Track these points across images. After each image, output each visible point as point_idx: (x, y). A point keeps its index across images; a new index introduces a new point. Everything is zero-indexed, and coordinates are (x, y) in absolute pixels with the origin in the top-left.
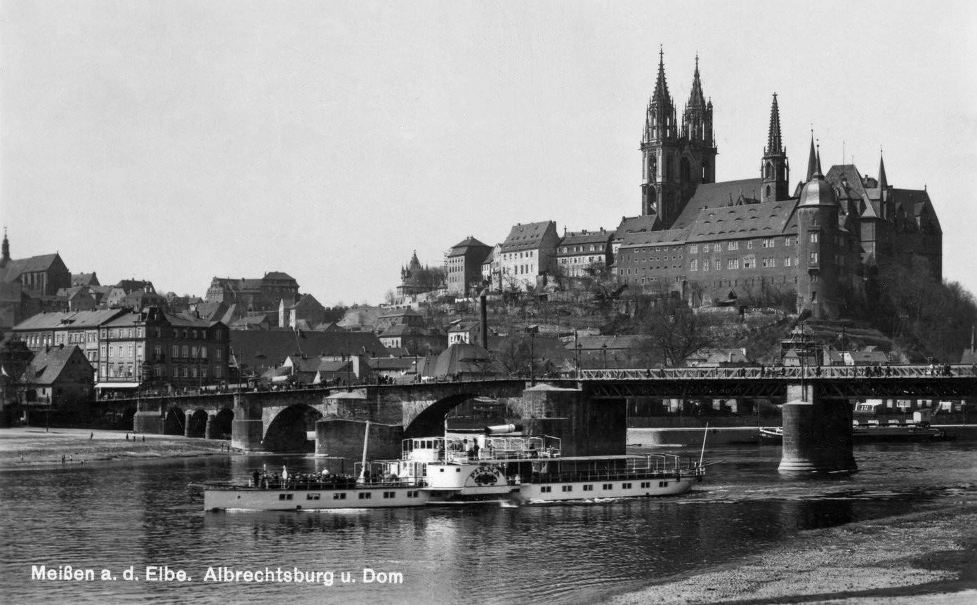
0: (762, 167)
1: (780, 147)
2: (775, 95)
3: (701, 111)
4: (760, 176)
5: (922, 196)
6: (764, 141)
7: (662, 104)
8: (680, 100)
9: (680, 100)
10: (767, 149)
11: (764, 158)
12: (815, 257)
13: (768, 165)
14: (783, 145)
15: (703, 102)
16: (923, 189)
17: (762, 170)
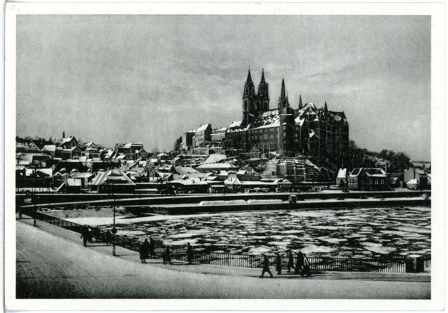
0: (279, 104)
1: (285, 97)
2: (283, 80)
3: (264, 87)
4: (278, 108)
5: (342, 115)
6: (279, 95)
7: (249, 83)
8: (257, 82)
9: (257, 82)
10: (280, 97)
11: (279, 101)
12: (285, 135)
13: (280, 103)
14: (286, 96)
15: (265, 83)
16: (342, 111)
17: (279, 105)
